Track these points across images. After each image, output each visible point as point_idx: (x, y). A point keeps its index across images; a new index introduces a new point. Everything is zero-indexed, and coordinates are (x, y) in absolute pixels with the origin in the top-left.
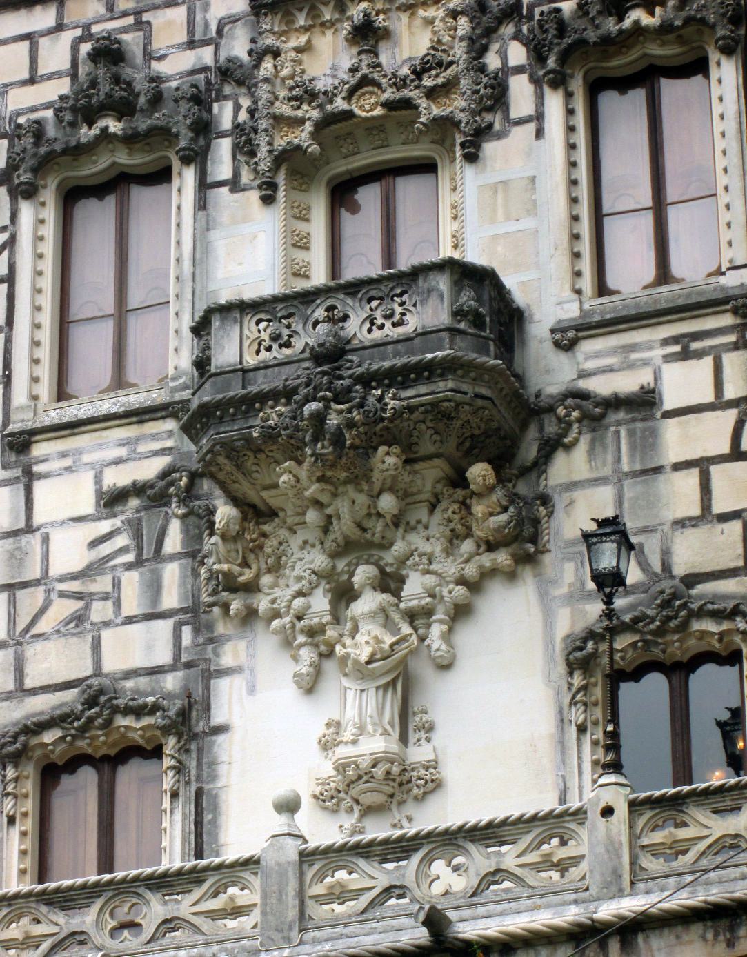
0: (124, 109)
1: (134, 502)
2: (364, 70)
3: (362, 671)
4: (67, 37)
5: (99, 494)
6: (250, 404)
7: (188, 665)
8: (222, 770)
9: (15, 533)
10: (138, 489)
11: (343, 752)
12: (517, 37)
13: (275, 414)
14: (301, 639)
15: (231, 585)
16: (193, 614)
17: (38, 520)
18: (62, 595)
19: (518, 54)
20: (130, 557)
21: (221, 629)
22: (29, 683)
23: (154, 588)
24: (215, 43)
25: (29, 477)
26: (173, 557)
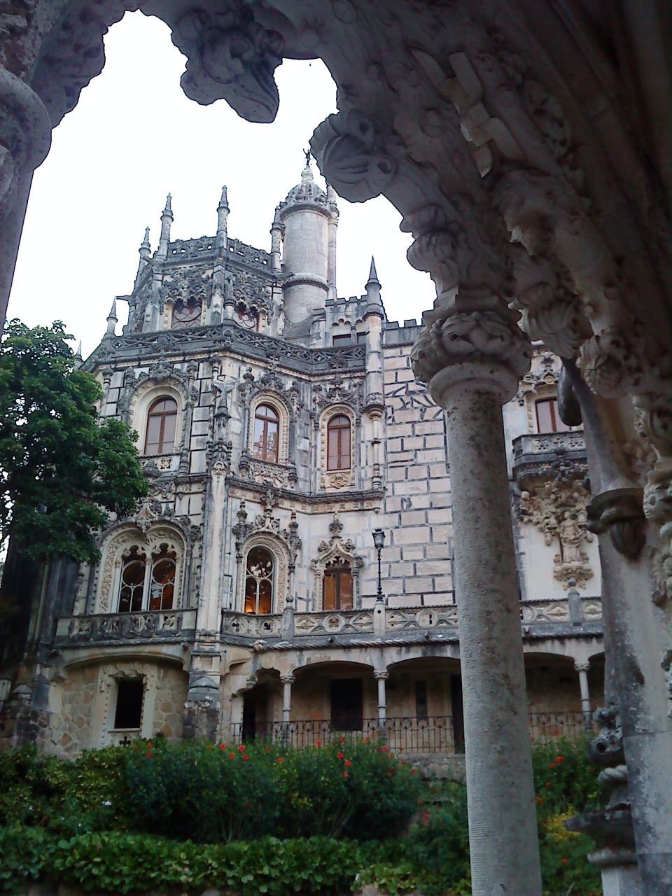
2: (548, 371)
3: (572, 542)
6: (538, 464)
8: (524, 565)
11: (566, 565)
13: (545, 467)
14: (547, 530)
15: (524, 513)
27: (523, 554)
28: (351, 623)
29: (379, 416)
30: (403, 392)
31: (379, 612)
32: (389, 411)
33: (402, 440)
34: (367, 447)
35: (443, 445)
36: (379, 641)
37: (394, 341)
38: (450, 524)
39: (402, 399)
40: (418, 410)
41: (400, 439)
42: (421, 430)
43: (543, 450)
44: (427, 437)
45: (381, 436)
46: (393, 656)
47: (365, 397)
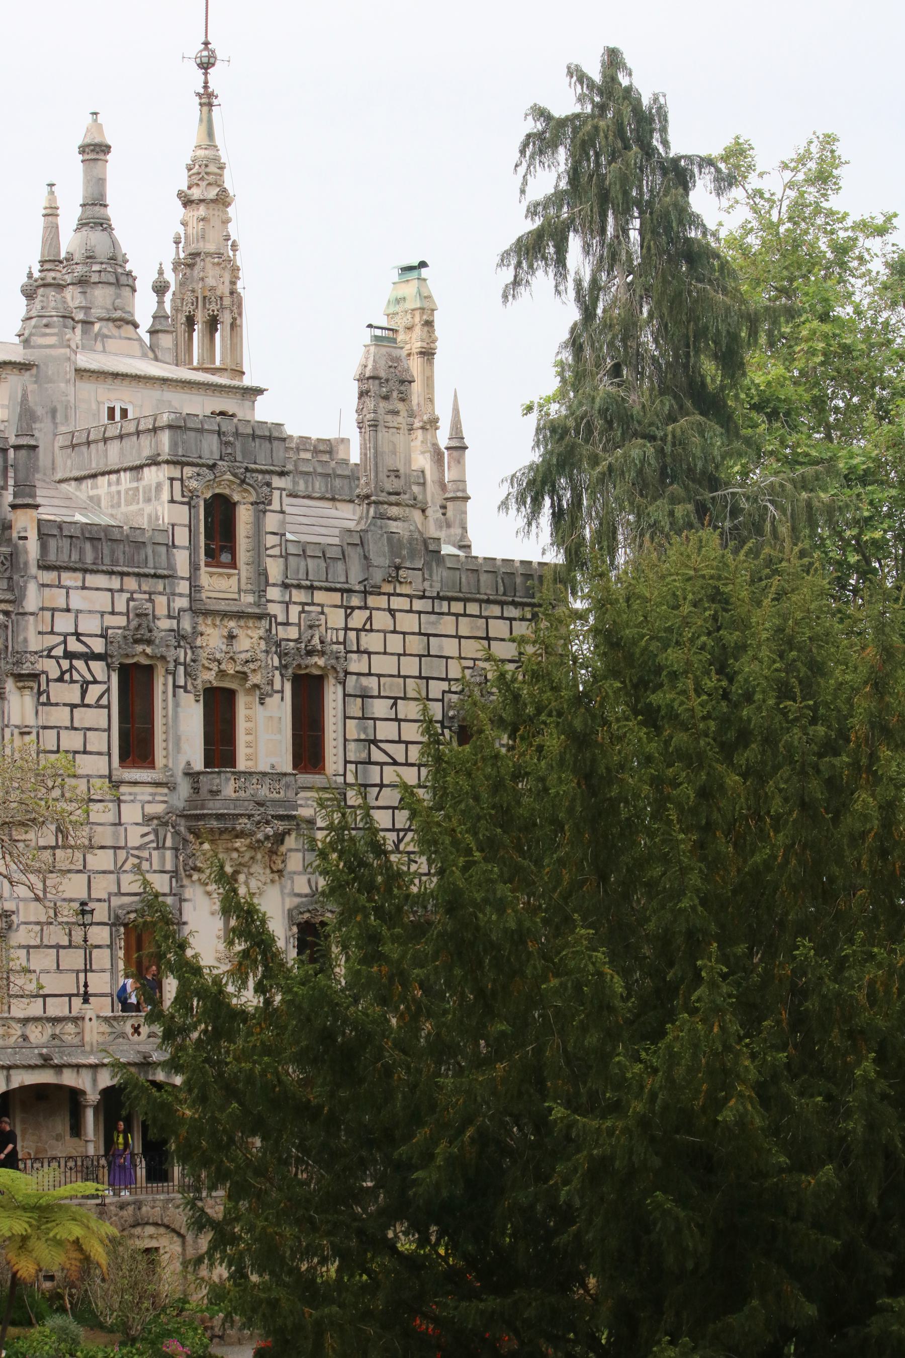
0: (149, 642)
1: (155, 822)
4: (127, 595)
5: (144, 815)
7: (175, 895)
9: (115, 824)
10: (158, 818)
12: (276, 653)
14: (215, 895)
16: (175, 874)
17: (123, 821)
18: (133, 855)
19: (276, 663)
20: (154, 845)
21: (186, 882)
22: (123, 891)
23: (163, 859)
24: (178, 618)
25: (119, 801)
26: (169, 848)
27: (185, 923)
28: (57, 1032)
29: (32, 688)
30: (59, 651)
31: (90, 1019)
32: (43, 678)
33: (58, 733)
34: (12, 735)
35: (105, 749)
36: (92, 1060)
37: (52, 557)
38: (111, 872)
39: (58, 662)
40: (78, 686)
41: (55, 731)
42: (82, 719)
43: (242, 794)
44: (89, 733)
45: (31, 720)
46: (105, 1080)
47: (10, 649)
